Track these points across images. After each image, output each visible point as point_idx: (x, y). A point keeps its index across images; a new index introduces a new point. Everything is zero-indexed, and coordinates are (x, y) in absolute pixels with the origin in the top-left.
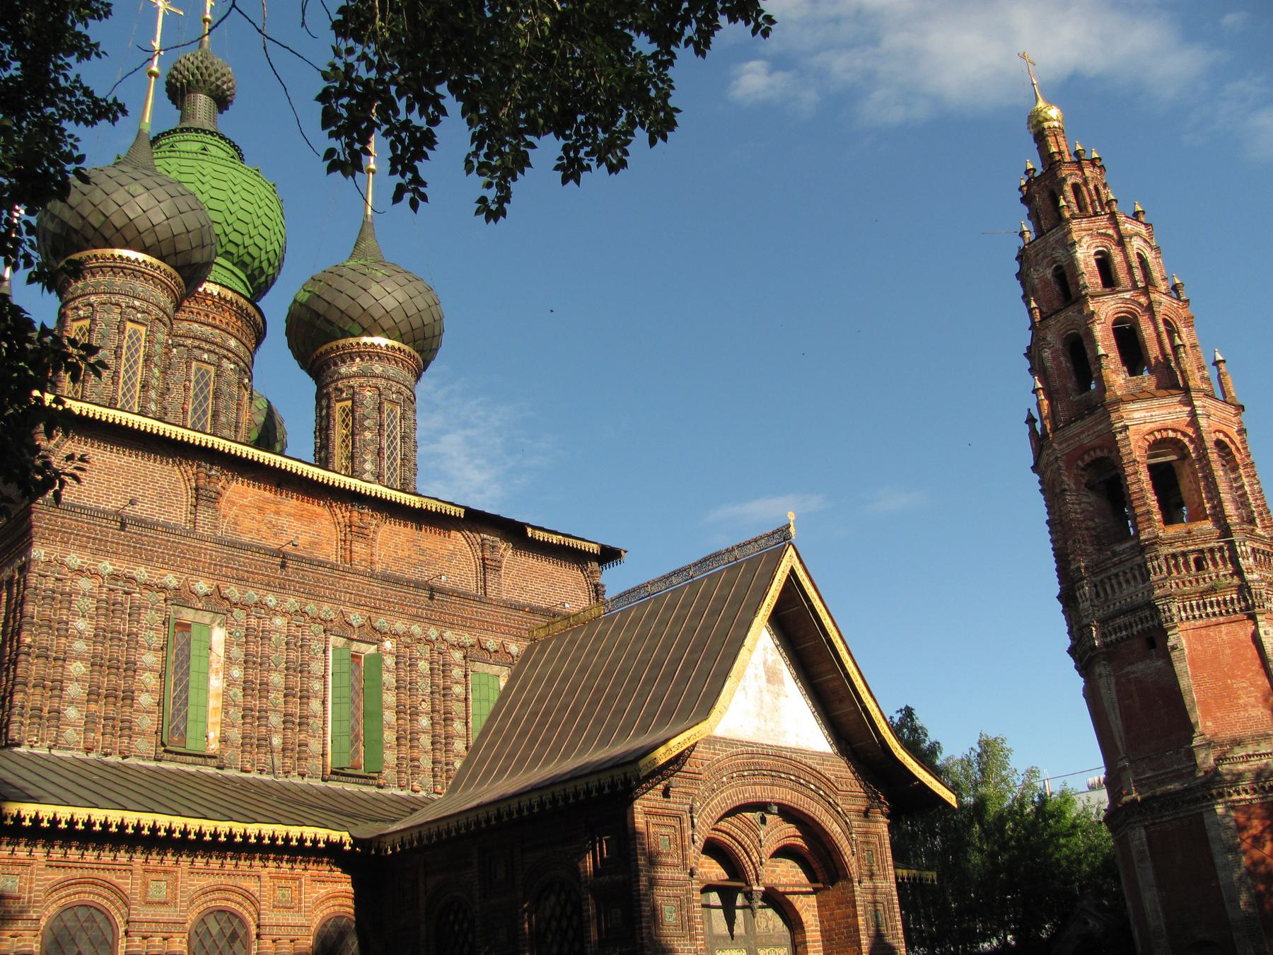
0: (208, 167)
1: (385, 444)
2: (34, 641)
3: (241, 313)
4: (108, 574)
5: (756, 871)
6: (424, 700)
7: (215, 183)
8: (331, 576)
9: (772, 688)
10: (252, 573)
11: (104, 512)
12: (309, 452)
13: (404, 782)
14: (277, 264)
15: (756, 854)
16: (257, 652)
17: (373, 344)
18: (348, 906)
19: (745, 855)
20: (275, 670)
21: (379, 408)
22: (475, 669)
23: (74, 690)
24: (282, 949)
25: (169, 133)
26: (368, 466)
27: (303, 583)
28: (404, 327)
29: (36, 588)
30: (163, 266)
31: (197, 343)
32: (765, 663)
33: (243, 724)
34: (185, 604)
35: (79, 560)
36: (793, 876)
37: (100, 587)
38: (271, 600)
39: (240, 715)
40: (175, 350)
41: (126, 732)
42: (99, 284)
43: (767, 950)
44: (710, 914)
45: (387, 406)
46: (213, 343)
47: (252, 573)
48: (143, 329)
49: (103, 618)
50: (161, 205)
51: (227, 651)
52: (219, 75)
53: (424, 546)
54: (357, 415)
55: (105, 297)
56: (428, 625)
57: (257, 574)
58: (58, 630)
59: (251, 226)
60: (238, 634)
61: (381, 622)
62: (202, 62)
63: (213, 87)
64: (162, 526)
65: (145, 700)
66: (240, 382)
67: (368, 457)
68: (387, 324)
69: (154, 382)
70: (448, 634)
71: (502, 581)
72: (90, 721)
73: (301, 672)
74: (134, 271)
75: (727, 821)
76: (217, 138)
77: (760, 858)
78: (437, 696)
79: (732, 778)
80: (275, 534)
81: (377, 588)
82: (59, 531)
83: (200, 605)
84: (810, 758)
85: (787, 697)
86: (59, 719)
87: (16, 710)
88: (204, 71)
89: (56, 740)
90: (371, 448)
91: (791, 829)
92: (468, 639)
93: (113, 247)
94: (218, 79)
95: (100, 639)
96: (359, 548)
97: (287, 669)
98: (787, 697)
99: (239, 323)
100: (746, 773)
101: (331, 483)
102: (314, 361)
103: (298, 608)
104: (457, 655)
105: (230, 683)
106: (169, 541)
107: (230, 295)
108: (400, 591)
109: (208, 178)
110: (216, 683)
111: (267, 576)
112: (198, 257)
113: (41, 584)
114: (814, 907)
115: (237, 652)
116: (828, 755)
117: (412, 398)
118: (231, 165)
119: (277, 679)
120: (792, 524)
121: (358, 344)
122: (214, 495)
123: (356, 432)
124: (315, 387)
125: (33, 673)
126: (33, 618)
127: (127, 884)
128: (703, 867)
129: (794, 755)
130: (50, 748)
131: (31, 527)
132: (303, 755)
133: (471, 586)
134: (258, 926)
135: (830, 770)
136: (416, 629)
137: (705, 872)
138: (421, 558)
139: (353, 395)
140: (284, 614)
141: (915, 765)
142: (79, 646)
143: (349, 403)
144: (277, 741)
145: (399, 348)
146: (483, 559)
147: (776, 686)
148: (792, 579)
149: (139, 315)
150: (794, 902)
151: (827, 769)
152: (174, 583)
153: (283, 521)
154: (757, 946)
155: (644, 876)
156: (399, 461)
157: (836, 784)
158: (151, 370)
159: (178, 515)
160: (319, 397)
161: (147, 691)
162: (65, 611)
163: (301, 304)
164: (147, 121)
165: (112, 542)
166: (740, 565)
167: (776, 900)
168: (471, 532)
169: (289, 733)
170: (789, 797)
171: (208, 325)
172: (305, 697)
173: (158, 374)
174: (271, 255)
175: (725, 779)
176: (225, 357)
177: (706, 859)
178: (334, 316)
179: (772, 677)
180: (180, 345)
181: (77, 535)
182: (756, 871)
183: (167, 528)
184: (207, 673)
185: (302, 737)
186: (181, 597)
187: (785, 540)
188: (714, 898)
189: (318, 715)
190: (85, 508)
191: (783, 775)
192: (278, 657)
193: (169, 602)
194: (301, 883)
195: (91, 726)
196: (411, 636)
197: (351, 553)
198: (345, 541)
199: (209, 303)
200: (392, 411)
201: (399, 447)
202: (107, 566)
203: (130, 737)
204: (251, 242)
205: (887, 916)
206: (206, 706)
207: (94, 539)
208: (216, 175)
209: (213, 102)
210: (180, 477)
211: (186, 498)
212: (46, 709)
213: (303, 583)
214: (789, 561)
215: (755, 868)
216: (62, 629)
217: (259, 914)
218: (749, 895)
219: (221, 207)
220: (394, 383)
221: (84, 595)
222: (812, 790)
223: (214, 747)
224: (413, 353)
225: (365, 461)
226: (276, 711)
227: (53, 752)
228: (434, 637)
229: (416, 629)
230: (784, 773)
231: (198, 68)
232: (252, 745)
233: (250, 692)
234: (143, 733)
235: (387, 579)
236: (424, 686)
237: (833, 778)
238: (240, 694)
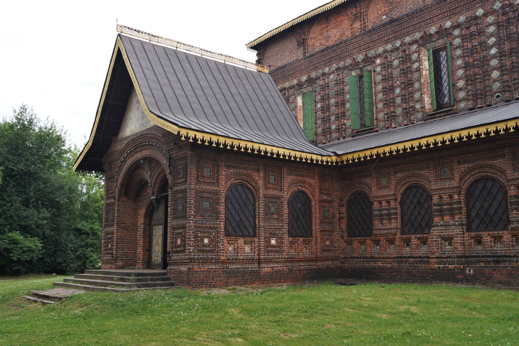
8: (346, 46)
38: (327, 70)
61: (372, 53)
108: (378, 33)
138: (391, 7)
140: (333, 72)
215: (154, 186)
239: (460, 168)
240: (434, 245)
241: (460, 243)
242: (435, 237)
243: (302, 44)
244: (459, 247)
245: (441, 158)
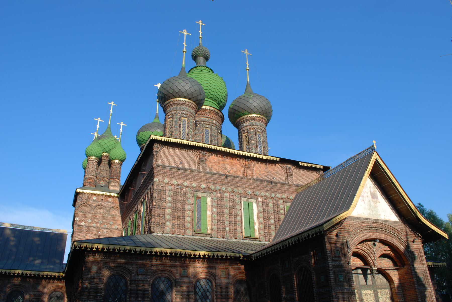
0: (203, 75)
1: (258, 144)
2: (157, 204)
3: (216, 113)
4: (176, 184)
5: (373, 263)
6: (272, 215)
7: (205, 79)
9: (373, 200)
10: (217, 181)
11: (174, 167)
12: (238, 148)
13: (267, 240)
14: (225, 99)
15: (373, 257)
16: (220, 204)
17: (252, 116)
18: (244, 277)
19: (369, 257)
20: (226, 209)
21: (255, 134)
22: (287, 205)
23: (168, 217)
24: (223, 290)
25: (193, 68)
26: (253, 151)
27: (233, 183)
28: (260, 110)
29: (156, 189)
30: (190, 101)
31: (204, 123)
32: (370, 192)
33: (217, 224)
34: (199, 191)
35: (167, 181)
36: (388, 264)
37: (174, 188)
38: (224, 188)
39: (216, 222)
40: (199, 125)
41: (183, 228)
42: (174, 108)
43: (381, 290)
44: (358, 277)
45: (257, 133)
46: (209, 122)
47: (217, 181)
48: (186, 119)
49: (175, 197)
50: (188, 85)
51: (211, 204)
52: (204, 51)
53: (268, 170)
54: (249, 137)
55: (175, 112)
56: (271, 193)
57: (219, 181)
58: (163, 200)
59: (216, 89)
60: (214, 199)
61: (257, 193)
62: (200, 48)
63: (203, 54)
64: (190, 170)
65: (188, 219)
66: (218, 132)
67: (253, 148)
68: (255, 110)
69: (191, 133)
70: (278, 195)
71: (293, 178)
72: (173, 225)
73: (234, 209)
74: (183, 104)
75: (360, 245)
76: (205, 68)
77: (375, 258)
78: (275, 213)
79: (361, 230)
80: (224, 170)
81: (255, 183)
82: (161, 173)
83: (203, 191)
84: (390, 223)
85: (379, 203)
86: (164, 225)
87: (152, 223)
88: (200, 50)
89: (164, 231)
90: (254, 145)
91: (386, 248)
92: (284, 196)
93: (176, 98)
94: (204, 52)
95: (175, 202)
96: (249, 172)
97: (229, 208)
98: (379, 203)
99: (216, 116)
100: (366, 229)
101: (238, 154)
102: (236, 123)
103: (232, 190)
104: (281, 201)
105: (213, 213)
106: (192, 174)
107: (212, 109)
109: (203, 78)
110: (209, 213)
111: (222, 182)
112: (200, 98)
113: (157, 188)
114: (397, 275)
115: (214, 204)
116: (397, 222)
117: (265, 130)
118: (209, 73)
119: (226, 211)
120: (375, 144)
121: (248, 117)
122: (205, 160)
123: (249, 141)
124: (238, 131)
125: (157, 213)
126: (156, 198)
127: (175, 271)
128: (354, 262)
129: (384, 222)
130: (162, 233)
131: (154, 173)
132: (236, 233)
133: (284, 180)
134: (216, 283)
135: (398, 227)
136: (268, 194)
139: (248, 131)
140: (228, 192)
141: (430, 224)
142: (169, 205)
143: (247, 134)
144: (228, 229)
145: (259, 117)
146: (287, 173)
147: (375, 199)
148: (376, 164)
149: (185, 115)
150: (389, 273)
151: (397, 227)
152: (195, 185)
153: (226, 166)
154: (377, 288)
155: (331, 264)
156: (262, 148)
157: (401, 232)
158: (189, 130)
159: (195, 166)
160: (239, 133)
161: (189, 216)
162: (164, 195)
163: (231, 108)
164: (184, 64)
165: (177, 175)
166: (358, 160)
167: (381, 271)
168: (282, 164)
169: (231, 226)
170: (383, 237)
171: (207, 118)
172: (235, 216)
173: (191, 131)
174: (223, 97)
175: (358, 231)
176: (213, 126)
177: (355, 258)
178: (240, 110)
179: (374, 196)
180: (200, 124)
181: (167, 174)
182: (373, 263)
183: (192, 170)
184: (206, 211)
185: (235, 227)
186: (197, 189)
187: (373, 150)
188: (360, 271)
189: (240, 221)
190: (168, 166)
191: (380, 229)
192: (227, 204)
193: (194, 191)
194: (228, 270)
195: (173, 227)
196: (266, 196)
197: (246, 173)
198: (244, 170)
199: (207, 111)
200: (259, 134)
201: (262, 145)
202: (175, 182)
203: (185, 230)
204: (217, 94)
205: (425, 278)
206: (207, 220)
207: (172, 175)
208: (205, 77)
209: (204, 59)
210: (195, 156)
211: (197, 161)
212: (161, 223)
213: (233, 183)
214: (375, 157)
215: (373, 261)
216: (164, 200)
217: (216, 280)
218: (372, 271)
219: (207, 85)
220: (259, 127)
221: (170, 190)
222: (392, 234)
223: (209, 231)
224: (264, 117)
225: (252, 149)
226: (227, 220)
227: (163, 235)
228: (273, 196)
229: (268, 194)
230: (381, 228)
231: (199, 50)
232: (220, 230)
233: (219, 215)
234: (188, 228)
235: (258, 180)
236: (271, 211)
237: (399, 230)
238: (216, 216)
243: (202, 161)
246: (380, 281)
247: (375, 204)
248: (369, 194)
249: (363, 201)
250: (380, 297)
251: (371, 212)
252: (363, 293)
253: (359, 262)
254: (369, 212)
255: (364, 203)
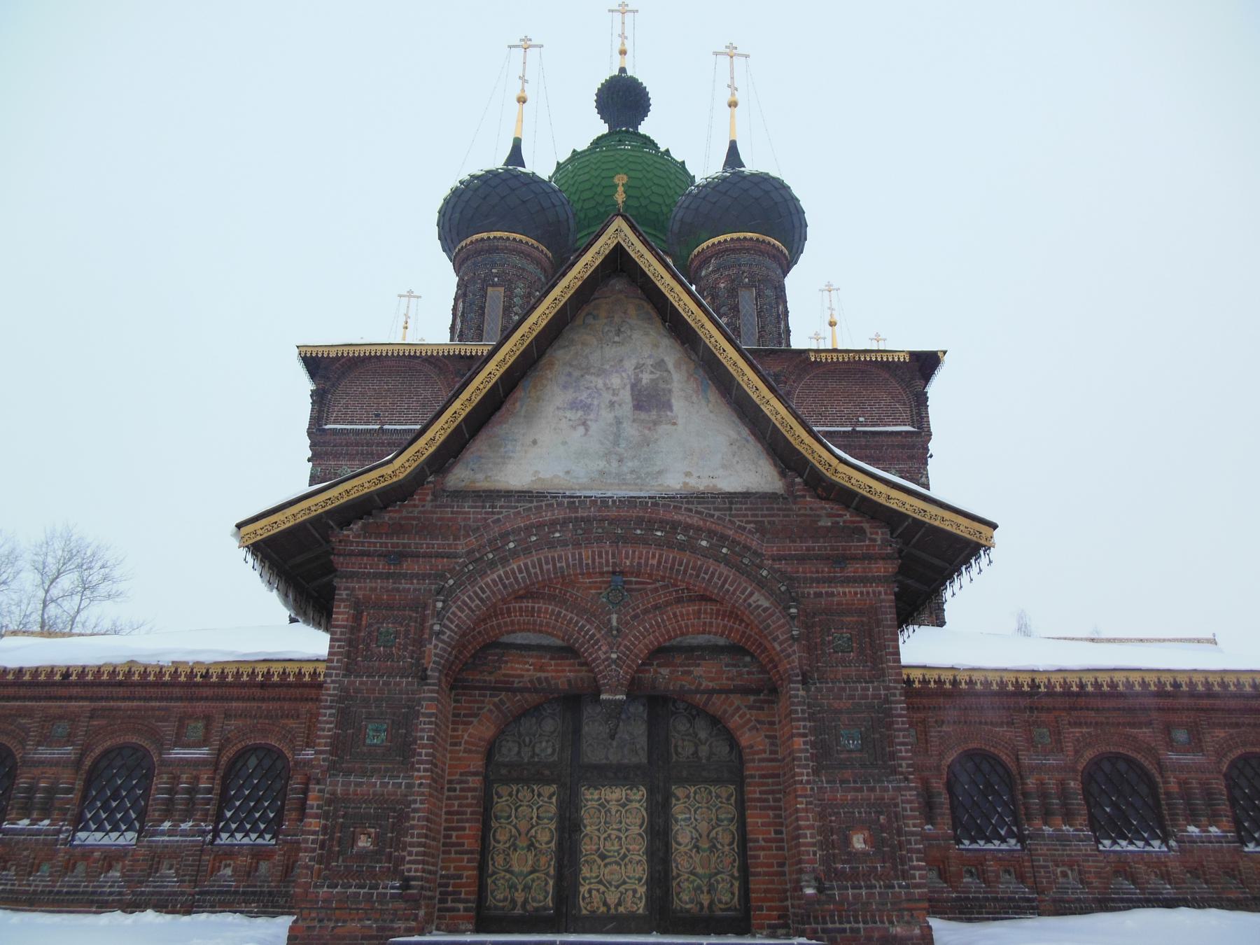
9: (643, 416)
32: (633, 386)
36: (728, 679)
43: (693, 790)
84: (699, 503)
85: (674, 424)
137: (546, 678)
147: (654, 412)
155: (333, 682)
239: (1072, 732)
240: (1043, 873)
241: (1095, 872)
242: (1041, 858)
244: (1094, 880)
245: (1037, 709)
246: (692, 750)
247: (647, 432)
248: (626, 395)
249: (584, 424)
250: (680, 817)
251: (615, 464)
252: (589, 797)
253: (570, 671)
254: (602, 464)
255: (585, 434)
